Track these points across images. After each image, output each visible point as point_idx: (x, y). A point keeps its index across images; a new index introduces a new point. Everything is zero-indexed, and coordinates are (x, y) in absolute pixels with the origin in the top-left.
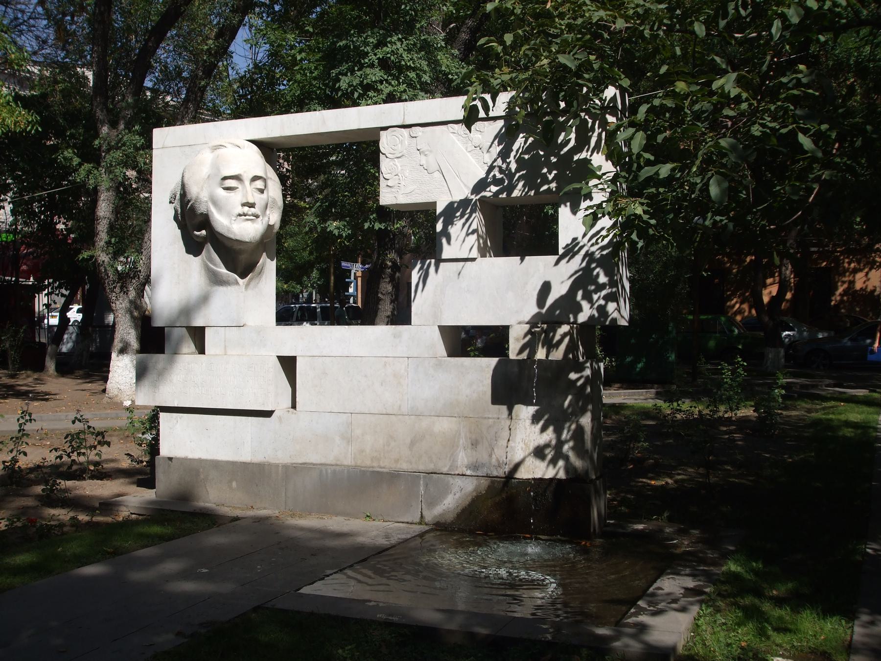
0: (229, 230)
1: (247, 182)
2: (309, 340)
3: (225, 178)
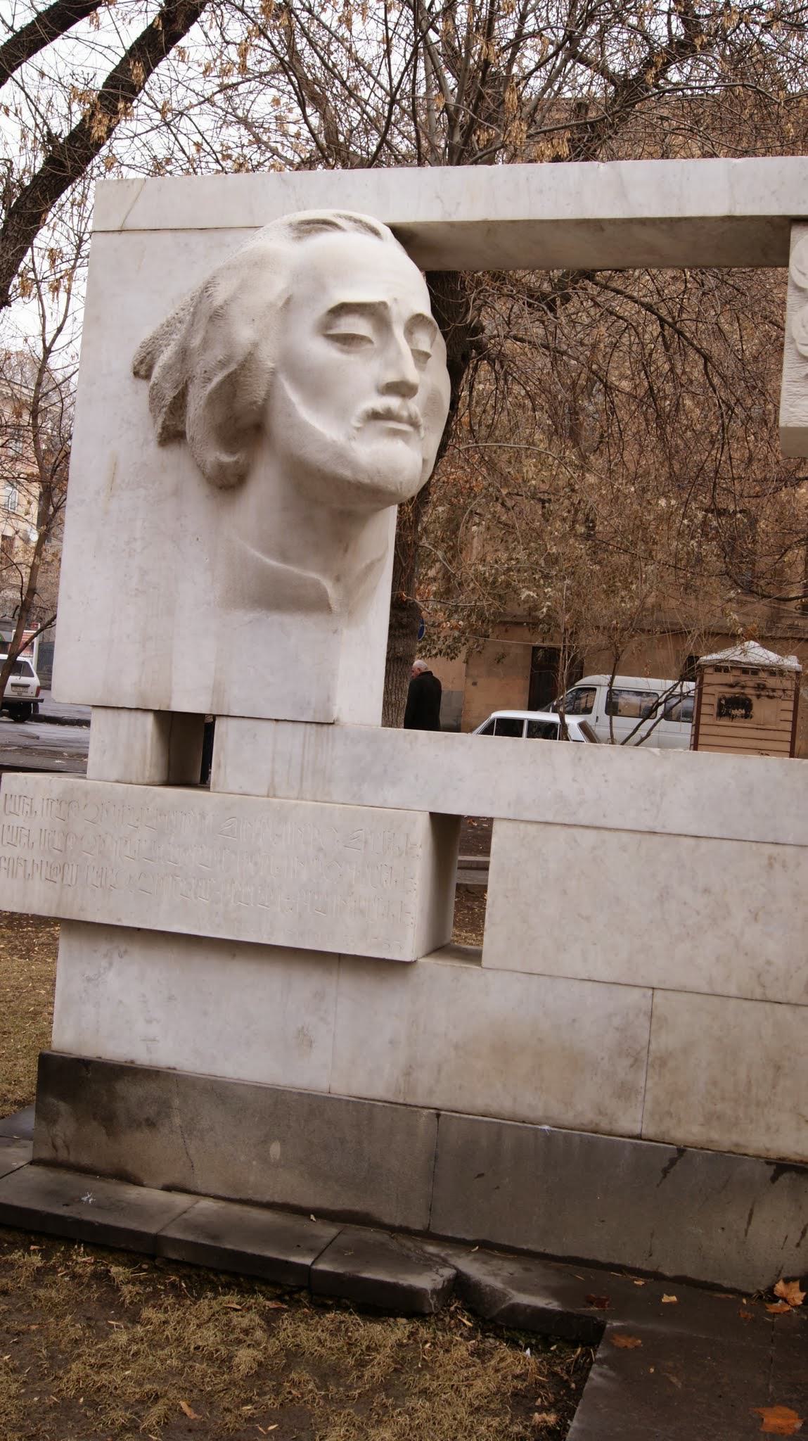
0: (341, 456)
1: (399, 332)
2: (464, 769)
3: (343, 309)
